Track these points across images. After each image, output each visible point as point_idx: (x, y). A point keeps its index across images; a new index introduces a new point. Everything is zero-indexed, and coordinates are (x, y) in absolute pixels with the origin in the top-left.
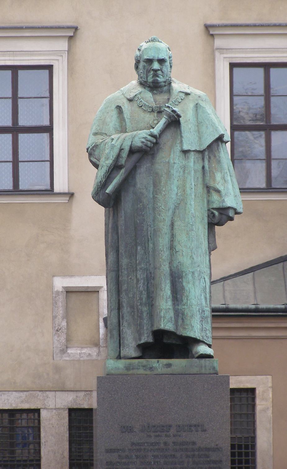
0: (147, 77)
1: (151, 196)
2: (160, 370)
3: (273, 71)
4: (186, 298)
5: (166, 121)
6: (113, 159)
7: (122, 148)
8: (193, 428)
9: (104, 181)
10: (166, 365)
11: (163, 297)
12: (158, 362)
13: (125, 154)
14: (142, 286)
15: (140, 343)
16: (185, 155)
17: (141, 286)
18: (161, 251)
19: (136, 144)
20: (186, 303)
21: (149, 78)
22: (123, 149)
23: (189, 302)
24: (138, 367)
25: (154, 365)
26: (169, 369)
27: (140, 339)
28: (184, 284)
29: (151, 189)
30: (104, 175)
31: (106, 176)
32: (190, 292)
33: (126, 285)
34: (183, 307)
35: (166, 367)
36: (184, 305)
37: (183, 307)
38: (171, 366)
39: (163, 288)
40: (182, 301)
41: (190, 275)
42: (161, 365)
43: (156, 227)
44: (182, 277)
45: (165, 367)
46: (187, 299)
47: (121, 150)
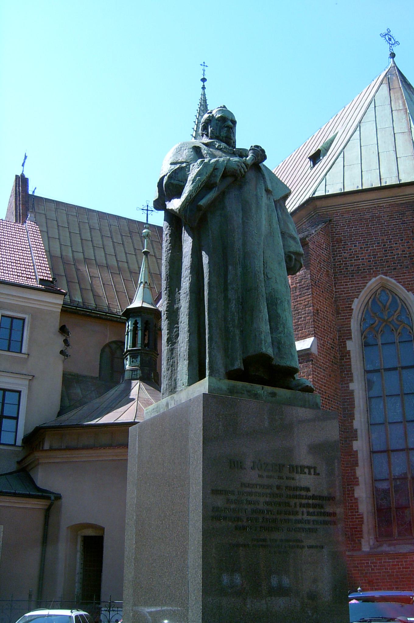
0: (220, 132)
1: (241, 221)
2: (265, 399)
3: (7, 393)
4: (282, 326)
5: (254, 159)
6: (207, 175)
7: (216, 167)
8: (306, 470)
9: (194, 196)
10: (270, 393)
11: (262, 320)
12: (263, 389)
13: (220, 174)
14: (235, 307)
15: (232, 369)
16: (267, 195)
17: (233, 307)
18: (258, 272)
19: (231, 166)
20: (282, 331)
21: (222, 133)
22: (217, 169)
23: (286, 330)
24: (243, 392)
25: (258, 392)
26: (274, 398)
27: (233, 365)
28: (279, 311)
29: (241, 215)
30: (195, 189)
31: (197, 190)
32: (286, 320)
33: (215, 304)
34: (279, 335)
35: (271, 396)
36: (280, 333)
37: (279, 335)
38: (276, 395)
39: (261, 310)
40: (278, 329)
41: (286, 303)
42: (265, 392)
43: (248, 250)
44: (276, 305)
45: (270, 395)
46: (284, 327)
47: (215, 169)
